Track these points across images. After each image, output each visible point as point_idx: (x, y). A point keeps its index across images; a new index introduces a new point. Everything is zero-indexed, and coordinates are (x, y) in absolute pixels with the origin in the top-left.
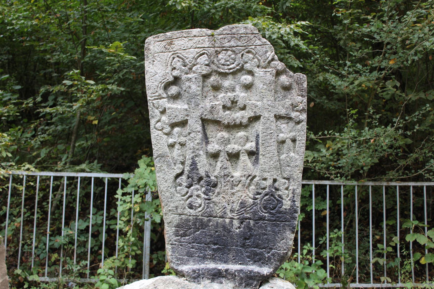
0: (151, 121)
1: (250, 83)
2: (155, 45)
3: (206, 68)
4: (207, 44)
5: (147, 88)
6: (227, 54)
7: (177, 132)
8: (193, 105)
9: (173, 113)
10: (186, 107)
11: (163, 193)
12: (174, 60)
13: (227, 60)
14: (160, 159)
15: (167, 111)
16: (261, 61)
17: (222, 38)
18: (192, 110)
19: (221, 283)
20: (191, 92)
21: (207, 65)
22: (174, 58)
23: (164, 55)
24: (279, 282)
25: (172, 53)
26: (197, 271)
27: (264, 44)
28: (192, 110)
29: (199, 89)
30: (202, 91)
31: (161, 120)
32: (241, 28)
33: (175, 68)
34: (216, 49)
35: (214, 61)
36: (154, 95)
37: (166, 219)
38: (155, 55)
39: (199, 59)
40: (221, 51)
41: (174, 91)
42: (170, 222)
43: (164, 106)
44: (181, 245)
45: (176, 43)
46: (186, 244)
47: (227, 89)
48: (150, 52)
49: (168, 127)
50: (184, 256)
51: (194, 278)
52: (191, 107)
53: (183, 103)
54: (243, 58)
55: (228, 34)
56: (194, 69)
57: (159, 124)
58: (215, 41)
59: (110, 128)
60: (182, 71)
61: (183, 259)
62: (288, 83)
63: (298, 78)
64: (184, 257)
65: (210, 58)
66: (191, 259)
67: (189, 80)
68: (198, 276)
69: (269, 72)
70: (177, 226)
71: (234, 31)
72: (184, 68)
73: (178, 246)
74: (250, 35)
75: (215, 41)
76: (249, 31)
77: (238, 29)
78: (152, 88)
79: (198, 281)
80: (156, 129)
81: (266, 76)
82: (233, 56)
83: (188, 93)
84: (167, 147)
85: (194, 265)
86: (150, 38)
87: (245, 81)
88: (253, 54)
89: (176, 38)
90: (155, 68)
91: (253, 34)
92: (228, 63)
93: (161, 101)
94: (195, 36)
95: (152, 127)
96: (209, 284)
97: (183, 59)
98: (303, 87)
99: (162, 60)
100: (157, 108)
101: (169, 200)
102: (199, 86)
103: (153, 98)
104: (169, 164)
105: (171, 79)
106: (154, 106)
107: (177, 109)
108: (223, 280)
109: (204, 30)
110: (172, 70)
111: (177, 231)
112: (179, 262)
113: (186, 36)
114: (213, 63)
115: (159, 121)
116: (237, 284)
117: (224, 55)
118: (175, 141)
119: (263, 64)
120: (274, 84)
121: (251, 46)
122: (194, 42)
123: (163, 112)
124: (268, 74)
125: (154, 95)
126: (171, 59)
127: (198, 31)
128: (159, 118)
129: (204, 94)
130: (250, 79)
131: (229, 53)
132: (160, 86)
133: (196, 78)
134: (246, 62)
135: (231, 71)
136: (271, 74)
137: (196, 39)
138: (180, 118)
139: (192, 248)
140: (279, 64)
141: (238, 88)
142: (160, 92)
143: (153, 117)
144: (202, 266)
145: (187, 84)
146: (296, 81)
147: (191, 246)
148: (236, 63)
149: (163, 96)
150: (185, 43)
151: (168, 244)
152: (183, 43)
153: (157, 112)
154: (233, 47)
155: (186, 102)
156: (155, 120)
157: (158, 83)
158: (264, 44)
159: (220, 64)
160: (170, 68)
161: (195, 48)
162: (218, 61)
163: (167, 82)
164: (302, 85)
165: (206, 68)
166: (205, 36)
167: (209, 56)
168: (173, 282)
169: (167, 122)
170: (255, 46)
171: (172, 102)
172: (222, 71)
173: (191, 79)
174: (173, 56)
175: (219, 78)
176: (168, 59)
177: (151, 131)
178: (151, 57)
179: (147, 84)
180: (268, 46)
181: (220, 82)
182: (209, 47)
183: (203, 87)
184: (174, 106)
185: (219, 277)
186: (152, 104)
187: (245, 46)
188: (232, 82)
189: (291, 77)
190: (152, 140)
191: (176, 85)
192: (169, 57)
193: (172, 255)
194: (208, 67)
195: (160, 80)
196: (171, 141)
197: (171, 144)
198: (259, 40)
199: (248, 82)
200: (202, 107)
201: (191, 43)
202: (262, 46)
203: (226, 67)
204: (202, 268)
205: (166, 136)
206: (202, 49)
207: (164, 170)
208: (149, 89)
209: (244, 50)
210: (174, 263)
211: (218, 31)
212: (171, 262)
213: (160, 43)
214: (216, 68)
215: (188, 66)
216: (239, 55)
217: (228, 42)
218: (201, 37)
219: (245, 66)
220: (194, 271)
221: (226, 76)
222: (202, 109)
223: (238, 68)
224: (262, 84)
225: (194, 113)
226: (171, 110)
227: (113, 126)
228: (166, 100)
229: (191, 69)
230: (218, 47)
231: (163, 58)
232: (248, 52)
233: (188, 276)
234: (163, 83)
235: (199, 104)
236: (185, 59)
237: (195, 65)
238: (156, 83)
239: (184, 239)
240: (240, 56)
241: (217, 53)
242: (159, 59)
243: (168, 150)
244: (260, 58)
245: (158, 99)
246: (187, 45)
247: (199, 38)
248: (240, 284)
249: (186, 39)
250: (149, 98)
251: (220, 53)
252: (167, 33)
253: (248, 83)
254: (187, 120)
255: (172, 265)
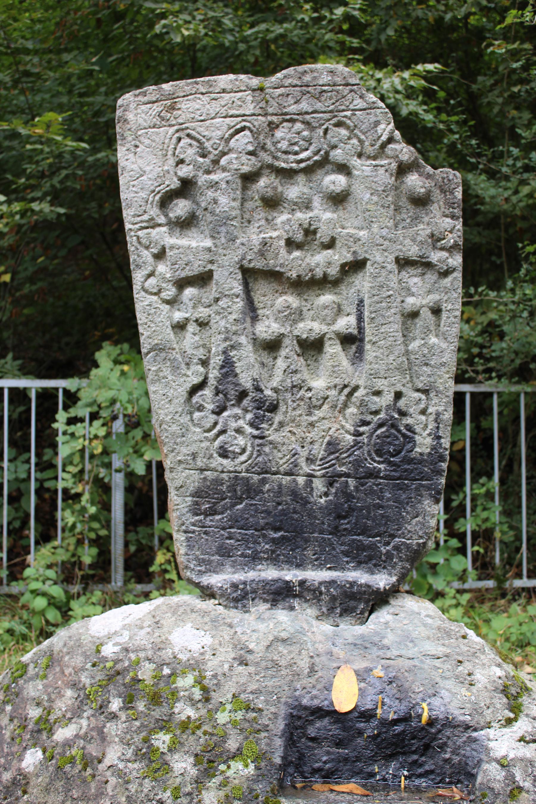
0: (134, 275)
1: (342, 191)
2: (139, 111)
3: (249, 160)
4: (249, 109)
5: (123, 204)
6: (293, 130)
7: (190, 296)
8: (223, 240)
9: (182, 256)
10: (208, 243)
11: (164, 426)
12: (181, 144)
13: (293, 142)
14: (157, 355)
15: (169, 253)
16: (367, 143)
17: (282, 95)
18: (220, 251)
19: (292, 608)
20: (218, 211)
21: (251, 153)
22: (179, 139)
23: (158, 134)
24: (409, 603)
25: (176, 128)
26: (241, 586)
27: (372, 107)
28: (220, 251)
29: (234, 204)
30: (241, 210)
31: (157, 273)
32: (322, 73)
33: (182, 161)
34: (269, 118)
35: (265, 144)
36: (139, 219)
37: (173, 479)
38: (139, 133)
39: (233, 140)
40: (281, 123)
41: (182, 210)
42: (181, 487)
43: (162, 243)
44: (206, 533)
45: (183, 106)
46: (216, 530)
47: (295, 204)
48: (129, 126)
49: (170, 286)
50: (213, 555)
51: (236, 600)
52: (219, 244)
53: (202, 236)
54: (328, 136)
55: (294, 86)
56: (223, 161)
57: (152, 281)
58: (267, 102)
59: (34, 288)
60: (197, 167)
61: (210, 562)
62: (423, 190)
63: (443, 178)
64: (212, 558)
65: (256, 139)
66: (228, 562)
67: (214, 185)
68: (244, 596)
69: (382, 166)
70: (197, 494)
71: (307, 78)
72: (201, 160)
73: (199, 534)
74: (341, 87)
75: (267, 102)
76: (338, 80)
77: (315, 74)
78: (135, 204)
79: (245, 606)
80: (146, 291)
81: (376, 176)
82: (305, 133)
83: (213, 213)
84: (169, 330)
85: (234, 573)
86: (127, 96)
87: (332, 187)
88: (348, 128)
89: (184, 96)
90: (140, 161)
91: (347, 85)
92: (296, 148)
93: (154, 233)
94: (224, 91)
95: (136, 287)
96: (268, 614)
97: (198, 141)
98: (455, 197)
99: (154, 144)
100: (147, 248)
101: (179, 440)
102: (234, 200)
103: (137, 226)
104: (175, 364)
105: (175, 184)
106: (140, 243)
107: (189, 248)
108: (296, 603)
109: (242, 77)
110: (177, 165)
111: (197, 504)
112: (203, 568)
113: (204, 91)
114: (263, 148)
115: (151, 274)
116: (324, 609)
117: (286, 131)
118: (187, 315)
119: (369, 150)
120: (393, 193)
121: (343, 111)
122: (223, 103)
123: (160, 256)
124: (382, 171)
125: (139, 219)
126: (174, 140)
127: (231, 81)
128: (150, 268)
129: (247, 216)
130: (342, 183)
131: (299, 126)
132: (151, 199)
133: (227, 182)
134: (335, 147)
135: (303, 165)
136: (386, 171)
137: (227, 96)
138: (196, 269)
139: (230, 538)
140: (405, 150)
141: (317, 202)
142: (152, 213)
143: (138, 266)
144: (251, 575)
145: (210, 194)
146: (440, 186)
147: (226, 535)
148: (312, 148)
149: (160, 222)
150: (204, 105)
151: (178, 531)
152: (197, 107)
153: (147, 255)
154: (307, 113)
155: (207, 232)
156: (143, 273)
157: (148, 193)
158: (372, 107)
159: (279, 150)
160: (172, 161)
161: (225, 117)
162: (275, 144)
163: (167, 192)
164: (452, 193)
165: (249, 160)
166: (245, 91)
167: (255, 134)
168: (192, 611)
169: (168, 275)
170: (353, 110)
171: (178, 235)
172: (283, 165)
173: (217, 183)
174: (177, 135)
175: (278, 180)
176: (167, 141)
177: (135, 296)
178: (130, 138)
179: (123, 196)
180: (379, 111)
181: (280, 189)
182: (254, 115)
183: (244, 200)
184: (183, 242)
185: (287, 596)
186: (135, 238)
187: (331, 112)
188: (306, 190)
189: (429, 176)
190: (138, 315)
191: (185, 198)
192: (168, 136)
193: (187, 554)
194: (253, 158)
195: (152, 188)
196: (178, 316)
197: (178, 322)
198: (361, 97)
199: (338, 189)
200: (243, 244)
201: (214, 107)
202: (368, 111)
203: (292, 157)
204: (252, 578)
205: (168, 307)
206: (240, 119)
207: (165, 377)
208: (129, 206)
209: (329, 120)
210: (193, 570)
211: (273, 79)
212: (187, 567)
213: (149, 106)
214: (269, 160)
215: (211, 157)
216: (318, 130)
217: (295, 103)
218: (236, 92)
219: (332, 153)
220: (235, 586)
221: (291, 177)
222: (244, 247)
223: (316, 158)
224: (369, 192)
225: (225, 255)
226: (177, 251)
227: (40, 284)
228: (164, 229)
229: (216, 162)
230: (273, 114)
231: (157, 140)
232: (339, 124)
233: (222, 596)
234: (159, 192)
235: (236, 238)
236: (204, 140)
237: (224, 154)
238: (143, 195)
239: (211, 520)
240: (322, 134)
241: (273, 127)
242: (147, 142)
243: (172, 336)
244: (363, 137)
245: (147, 228)
246: (208, 110)
247: (232, 95)
248: (331, 610)
249: (205, 98)
250: (128, 226)
251: (277, 127)
252: (164, 86)
253: (338, 191)
254: (211, 272)
255: (188, 574)
